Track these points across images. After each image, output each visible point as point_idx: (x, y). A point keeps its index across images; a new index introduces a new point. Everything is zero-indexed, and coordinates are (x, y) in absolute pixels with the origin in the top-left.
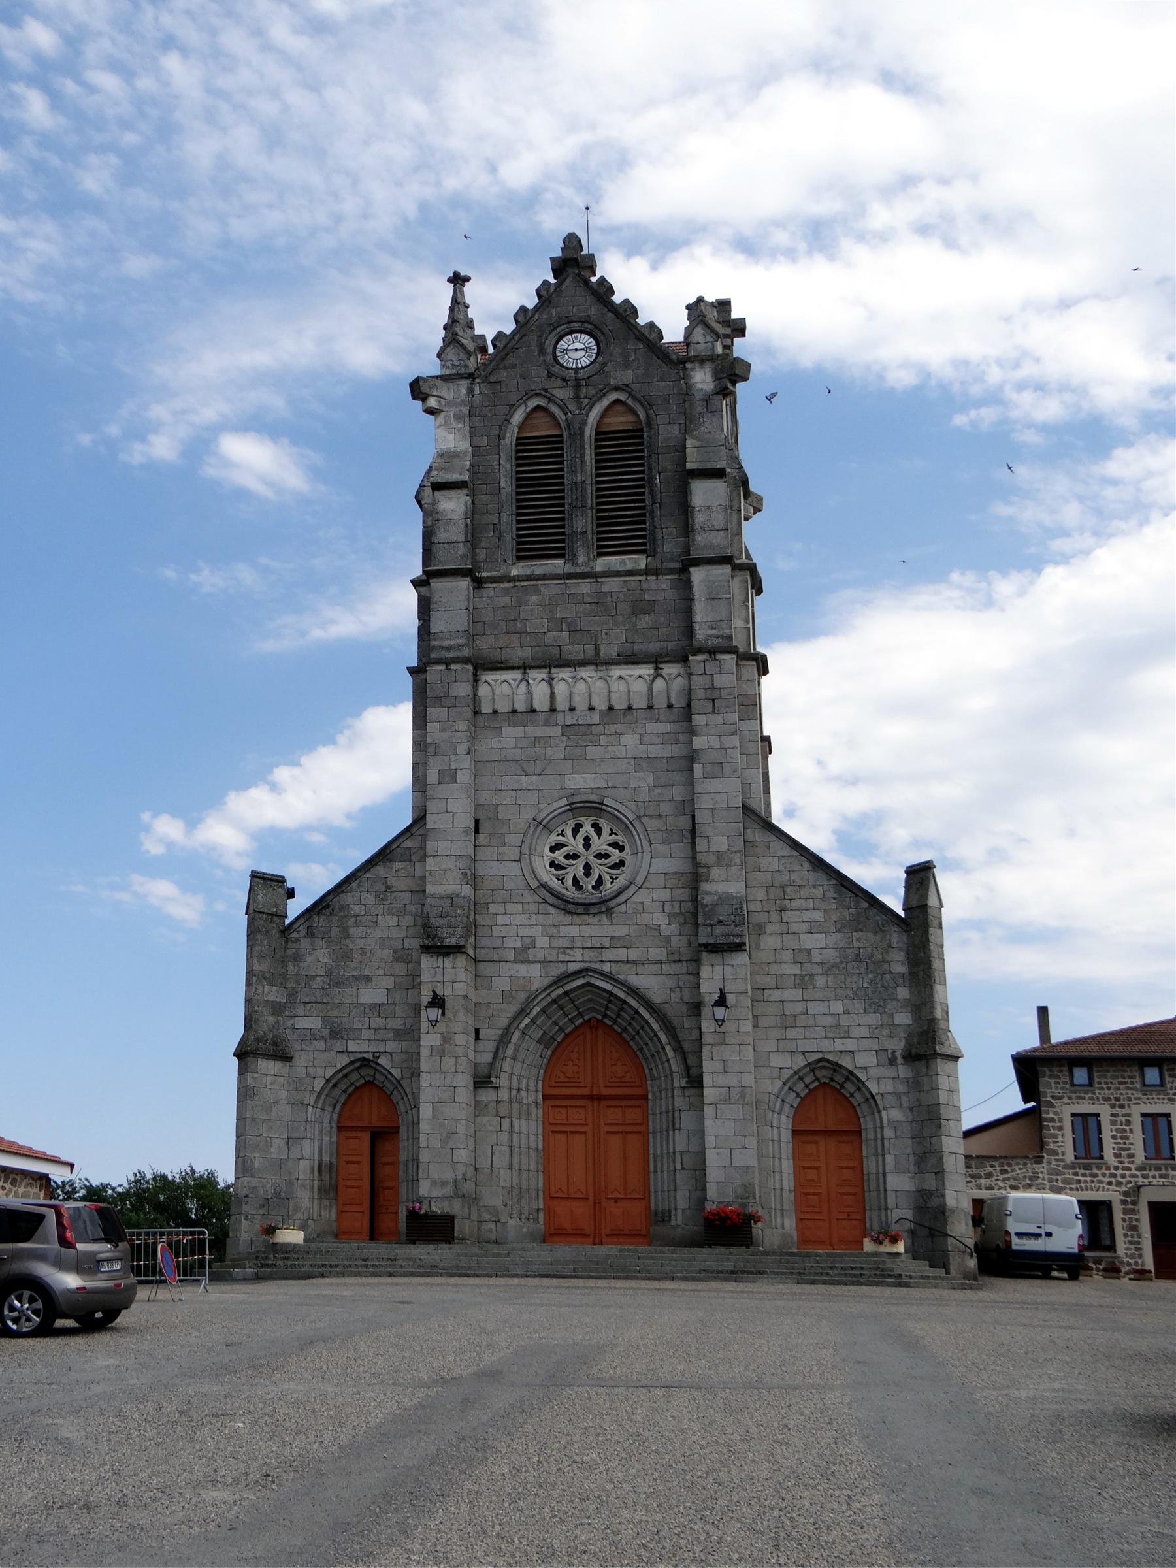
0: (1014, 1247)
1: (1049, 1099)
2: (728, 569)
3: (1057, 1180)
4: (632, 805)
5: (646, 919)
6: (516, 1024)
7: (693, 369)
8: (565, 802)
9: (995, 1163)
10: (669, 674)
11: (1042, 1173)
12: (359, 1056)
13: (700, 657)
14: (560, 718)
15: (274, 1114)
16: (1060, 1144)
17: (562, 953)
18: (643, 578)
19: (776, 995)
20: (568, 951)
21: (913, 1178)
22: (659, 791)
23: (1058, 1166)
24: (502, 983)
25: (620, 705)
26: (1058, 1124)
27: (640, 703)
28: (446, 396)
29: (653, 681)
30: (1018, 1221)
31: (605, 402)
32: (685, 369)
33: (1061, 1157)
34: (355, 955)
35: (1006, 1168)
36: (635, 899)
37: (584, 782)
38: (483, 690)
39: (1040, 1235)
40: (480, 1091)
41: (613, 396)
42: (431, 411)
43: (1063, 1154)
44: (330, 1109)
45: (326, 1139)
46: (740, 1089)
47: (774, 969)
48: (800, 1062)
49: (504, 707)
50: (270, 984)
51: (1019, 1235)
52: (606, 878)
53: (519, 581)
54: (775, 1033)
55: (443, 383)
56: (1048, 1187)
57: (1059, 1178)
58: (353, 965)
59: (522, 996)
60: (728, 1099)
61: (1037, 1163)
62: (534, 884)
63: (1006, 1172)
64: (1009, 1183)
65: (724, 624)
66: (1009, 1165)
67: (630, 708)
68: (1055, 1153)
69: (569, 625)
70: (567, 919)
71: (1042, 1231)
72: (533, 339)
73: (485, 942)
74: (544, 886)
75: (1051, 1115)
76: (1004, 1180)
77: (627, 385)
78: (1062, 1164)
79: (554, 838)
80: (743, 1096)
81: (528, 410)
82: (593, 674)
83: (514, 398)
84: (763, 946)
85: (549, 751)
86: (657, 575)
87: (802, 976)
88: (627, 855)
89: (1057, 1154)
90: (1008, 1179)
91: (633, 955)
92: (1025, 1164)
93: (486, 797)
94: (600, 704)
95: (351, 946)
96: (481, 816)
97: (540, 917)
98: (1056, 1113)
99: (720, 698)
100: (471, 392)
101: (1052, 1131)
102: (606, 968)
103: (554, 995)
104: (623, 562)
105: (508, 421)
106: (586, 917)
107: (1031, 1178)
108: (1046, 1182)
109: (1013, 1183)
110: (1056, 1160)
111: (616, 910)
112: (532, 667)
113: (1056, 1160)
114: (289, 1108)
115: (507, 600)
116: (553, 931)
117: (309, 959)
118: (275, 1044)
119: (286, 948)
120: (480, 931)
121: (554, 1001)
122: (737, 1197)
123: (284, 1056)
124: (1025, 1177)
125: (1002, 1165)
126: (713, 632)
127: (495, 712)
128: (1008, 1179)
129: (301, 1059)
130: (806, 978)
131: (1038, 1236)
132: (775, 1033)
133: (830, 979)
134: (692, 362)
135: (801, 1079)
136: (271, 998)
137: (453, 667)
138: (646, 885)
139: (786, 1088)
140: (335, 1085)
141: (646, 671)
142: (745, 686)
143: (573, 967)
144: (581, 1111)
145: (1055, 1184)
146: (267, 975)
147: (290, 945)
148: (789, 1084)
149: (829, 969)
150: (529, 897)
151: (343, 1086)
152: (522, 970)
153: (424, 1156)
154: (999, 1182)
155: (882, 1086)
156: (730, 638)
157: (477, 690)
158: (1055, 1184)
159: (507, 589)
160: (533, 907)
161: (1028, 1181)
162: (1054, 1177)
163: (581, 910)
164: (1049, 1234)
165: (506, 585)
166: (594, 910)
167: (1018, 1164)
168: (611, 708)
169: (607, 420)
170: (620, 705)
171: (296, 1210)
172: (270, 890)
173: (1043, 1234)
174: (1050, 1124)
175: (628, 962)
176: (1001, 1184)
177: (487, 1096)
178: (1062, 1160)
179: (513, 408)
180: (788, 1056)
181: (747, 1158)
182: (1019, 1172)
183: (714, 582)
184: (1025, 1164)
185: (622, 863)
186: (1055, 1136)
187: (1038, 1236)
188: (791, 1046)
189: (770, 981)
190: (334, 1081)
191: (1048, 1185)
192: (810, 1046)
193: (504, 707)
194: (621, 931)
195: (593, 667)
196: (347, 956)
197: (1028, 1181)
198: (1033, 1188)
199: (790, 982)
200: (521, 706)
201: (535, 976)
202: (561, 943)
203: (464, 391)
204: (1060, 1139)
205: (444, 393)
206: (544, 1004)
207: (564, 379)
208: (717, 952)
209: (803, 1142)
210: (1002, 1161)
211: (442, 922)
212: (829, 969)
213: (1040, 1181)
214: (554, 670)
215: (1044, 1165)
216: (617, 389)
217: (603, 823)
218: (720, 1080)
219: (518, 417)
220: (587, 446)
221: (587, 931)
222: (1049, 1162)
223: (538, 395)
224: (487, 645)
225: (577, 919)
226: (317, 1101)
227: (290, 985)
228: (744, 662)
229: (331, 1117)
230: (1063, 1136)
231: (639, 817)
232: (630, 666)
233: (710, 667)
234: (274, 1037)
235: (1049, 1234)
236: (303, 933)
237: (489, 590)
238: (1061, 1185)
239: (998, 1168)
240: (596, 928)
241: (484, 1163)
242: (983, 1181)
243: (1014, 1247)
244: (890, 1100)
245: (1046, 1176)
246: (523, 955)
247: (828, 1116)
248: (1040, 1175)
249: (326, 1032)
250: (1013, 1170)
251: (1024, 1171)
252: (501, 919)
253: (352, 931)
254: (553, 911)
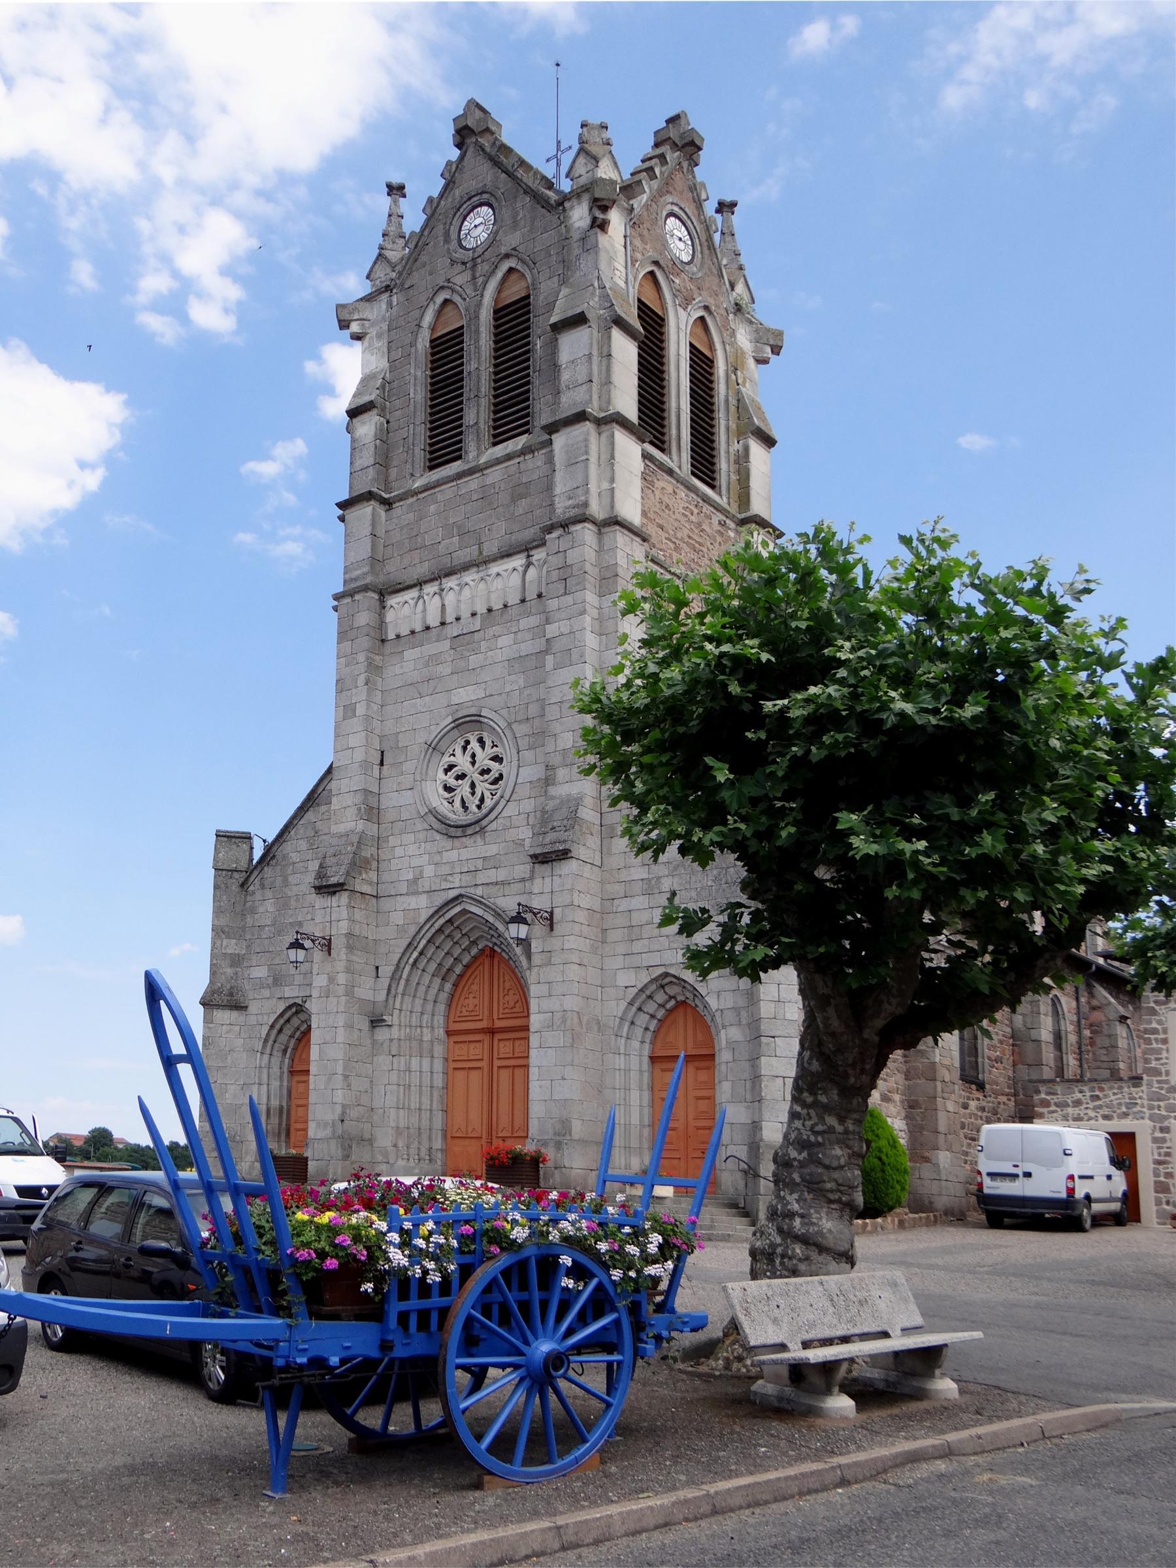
0: (986, 1191)
1: (1152, 1005)
2: (588, 426)
3: (1159, 1107)
4: (504, 712)
5: (512, 834)
6: (405, 959)
7: (572, 207)
8: (450, 719)
9: (1085, 1088)
10: (539, 560)
11: (1141, 1098)
12: (291, 1001)
13: (555, 534)
14: (448, 629)
15: (229, 1060)
16: (1164, 1061)
17: (446, 880)
18: (522, 459)
19: (623, 905)
20: (449, 878)
21: (748, 1107)
22: (527, 692)
23: (1161, 1088)
24: (397, 918)
25: (497, 606)
26: (1162, 1036)
27: (513, 599)
28: (370, 317)
29: (525, 572)
30: (989, 1158)
31: (499, 275)
32: (564, 210)
33: (1164, 1078)
34: (292, 903)
35: (1097, 1093)
36: (504, 814)
37: (465, 696)
38: (390, 616)
39: (1017, 1176)
40: (377, 1030)
41: (505, 267)
42: (357, 337)
43: (1167, 1073)
44: (280, 1054)
45: (275, 1084)
46: (561, 1014)
47: (624, 875)
48: (644, 978)
49: (405, 631)
50: (228, 937)
51: (992, 1175)
52: (487, 794)
53: (420, 493)
54: (622, 949)
55: (367, 304)
56: (1147, 1115)
57: (1161, 1103)
58: (291, 912)
59: (413, 930)
60: (550, 1026)
61: (1135, 1086)
62: (425, 810)
63: (1098, 1098)
64: (1102, 1112)
65: (580, 491)
66: (1101, 1089)
67: (505, 606)
68: (1157, 1073)
69: (459, 528)
70: (448, 843)
71: (1019, 1171)
72: (440, 230)
73: (385, 877)
74: (433, 812)
75: (1154, 1025)
76: (1095, 1108)
77: (514, 249)
78: (1166, 1086)
79: (447, 760)
80: (564, 1021)
81: (437, 306)
82: (476, 576)
83: (422, 300)
84: (614, 851)
85: (440, 668)
86: (533, 452)
87: (649, 880)
88: (503, 768)
89: (1160, 1074)
90: (1100, 1107)
91: (502, 875)
92: (1120, 1088)
93: (390, 727)
94: (481, 609)
95: (289, 894)
96: (385, 748)
97: (428, 845)
98: (1159, 1022)
99: (572, 575)
100: (390, 305)
101: (1154, 1045)
102: (479, 891)
103: (437, 926)
104: (506, 448)
105: (419, 326)
106: (464, 839)
107: (1128, 1106)
108: (1145, 1110)
109: (1106, 1111)
110: (1159, 1082)
111: (488, 828)
112: (426, 582)
113: (1159, 1082)
114: (244, 1055)
115: (411, 515)
116: (437, 858)
117: (261, 910)
118: (231, 994)
119: (245, 902)
120: (383, 865)
121: (440, 930)
122: (555, 1134)
123: (240, 1007)
124: (1120, 1104)
125: (1092, 1089)
126: (570, 502)
127: (398, 636)
128: (1100, 1107)
129: (253, 1008)
130: (653, 882)
131: (1014, 1176)
132: (622, 949)
133: (676, 879)
134: (569, 199)
135: (650, 997)
136: (229, 951)
137: (357, 597)
138: (514, 797)
139: (634, 1009)
140: (280, 1031)
141: (518, 561)
142: (607, 557)
143: (452, 894)
144: (477, 1045)
145: (1156, 1111)
146: (226, 929)
147: (249, 898)
148: (637, 1005)
149: (675, 869)
150: (420, 825)
151: (288, 1031)
152: (414, 902)
153: (313, 1098)
154: (1089, 1111)
155: (722, 1001)
156: (586, 504)
157: (385, 616)
158: (1156, 1111)
159: (412, 504)
160: (422, 836)
161: (1124, 1109)
162: (1156, 1103)
163: (459, 832)
164: (1028, 1175)
165: (411, 500)
166: (470, 831)
167: (1111, 1088)
168: (490, 610)
169: (504, 294)
170: (497, 606)
171: (246, 1153)
172: (234, 847)
173: (1021, 1175)
174: (1152, 1037)
175: (497, 883)
176: (1092, 1114)
177: (382, 1034)
178: (1167, 1082)
179: (423, 309)
180: (632, 972)
181: (569, 1090)
182: (1113, 1098)
183: (573, 445)
184: (1120, 1088)
185: (501, 777)
186: (1159, 1051)
187: (1014, 1176)
188: (636, 961)
189: (619, 889)
190: (278, 1027)
191: (1147, 1113)
192: (655, 959)
193: (405, 631)
194: (492, 850)
195: (475, 569)
196: (286, 906)
197: (1124, 1109)
198: (1130, 1117)
199: (638, 888)
200: (418, 627)
201: (423, 905)
202: (445, 870)
203: (384, 306)
204: (1164, 1054)
205: (367, 314)
206: (429, 935)
207: (464, 263)
208: (547, 862)
209: (663, 1070)
210: (1094, 1084)
211: (334, 860)
212: (675, 869)
213: (1138, 1108)
214: (444, 581)
215: (1144, 1088)
216: (507, 256)
217: (485, 736)
218: (547, 1004)
219: (429, 318)
220: (482, 329)
221: (465, 854)
222: (1150, 1085)
223: (442, 288)
224: (395, 569)
225: (457, 842)
226: (264, 1047)
227: (248, 937)
228: (607, 529)
229: (282, 1062)
230: (1168, 1051)
231: (509, 724)
232: (506, 560)
233: (564, 544)
234: (232, 988)
235: (1028, 1175)
236: (257, 886)
237: (399, 509)
238: (1164, 1113)
239: (1088, 1094)
240: (472, 850)
241: (377, 1103)
242: (1070, 1110)
243: (986, 1191)
244: (729, 1017)
245: (1146, 1102)
246: (414, 887)
247: (682, 1043)
248: (1139, 1101)
249: (271, 980)
250: (1106, 1096)
251: (1120, 1096)
252: (399, 852)
253: (290, 879)
254: (438, 837)
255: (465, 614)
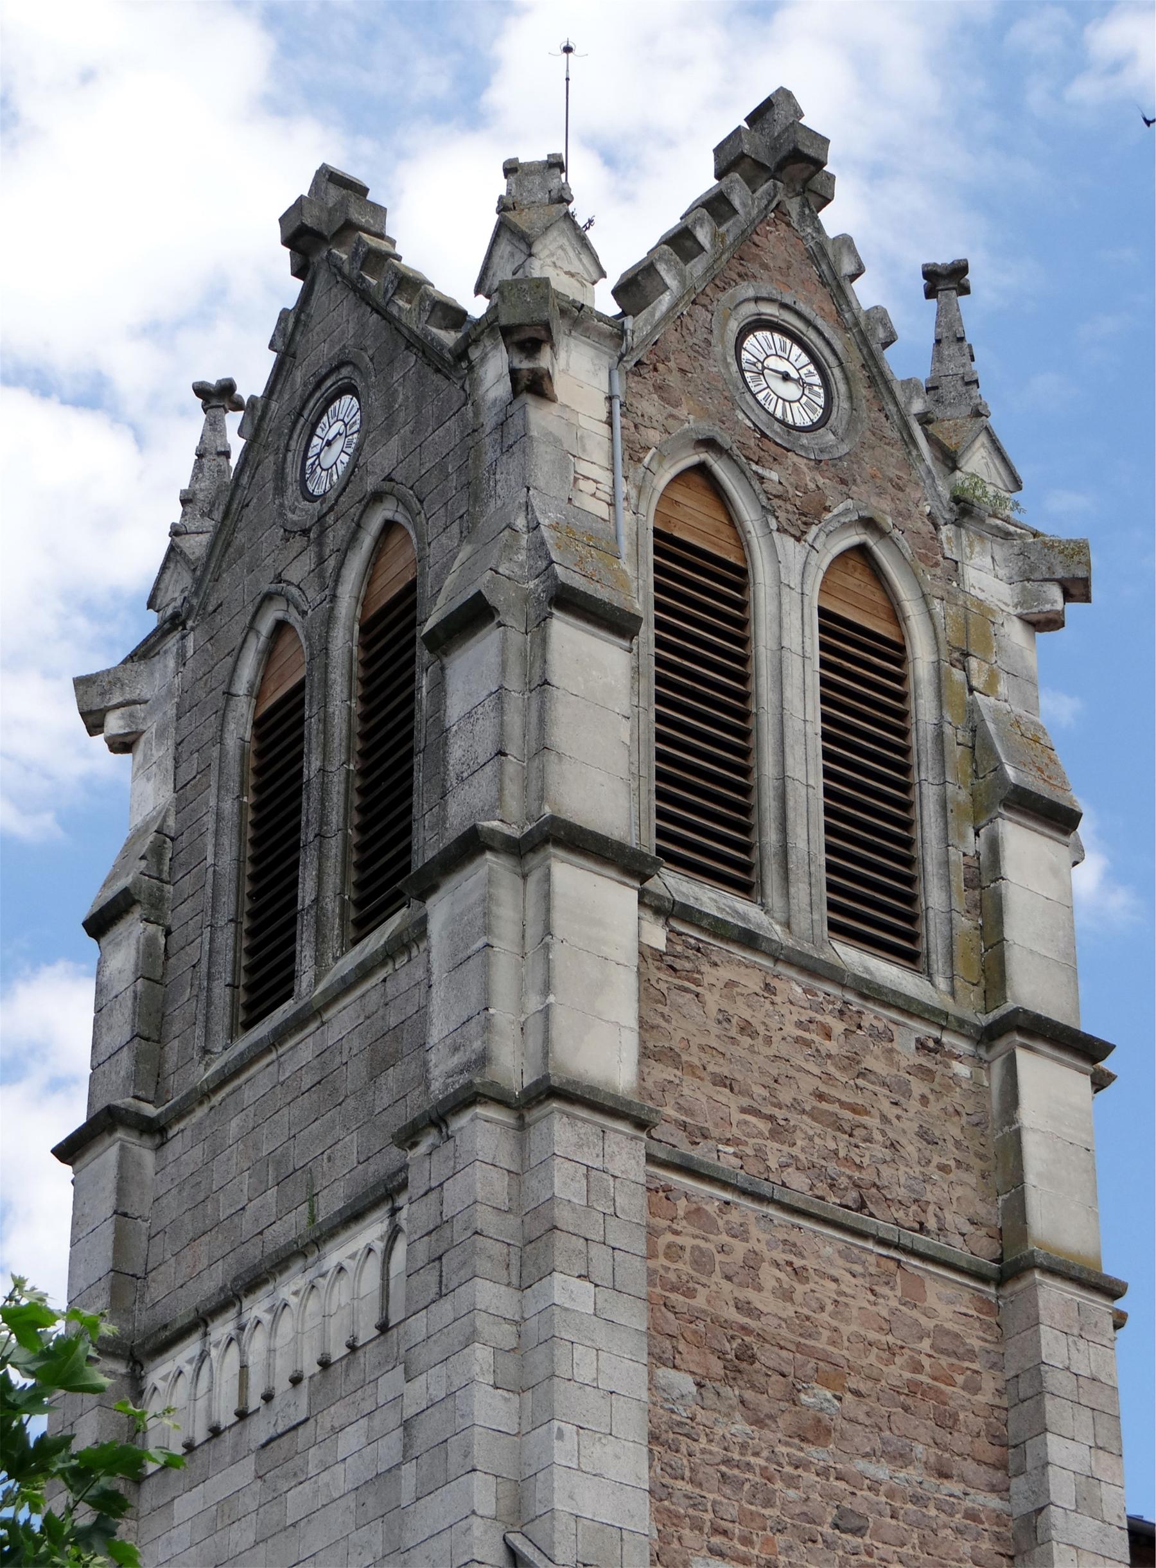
7: (483, 359)
18: (389, 969)
25: (338, 1351)
28: (147, 693)
31: (367, 541)
55: (142, 667)
65: (473, 1028)
72: (268, 469)
77: (389, 478)
85: (234, 1533)
134: (476, 341)
141: (373, 1231)
156: (483, 1059)
165: (200, 1112)
169: (380, 582)
179: (238, 654)
183: (462, 914)
203: (171, 663)
207: (305, 532)
216: (377, 497)
223: (269, 597)
228: (536, 1113)
232: (355, 1228)
233: (438, 1168)
255: (282, 1385)
